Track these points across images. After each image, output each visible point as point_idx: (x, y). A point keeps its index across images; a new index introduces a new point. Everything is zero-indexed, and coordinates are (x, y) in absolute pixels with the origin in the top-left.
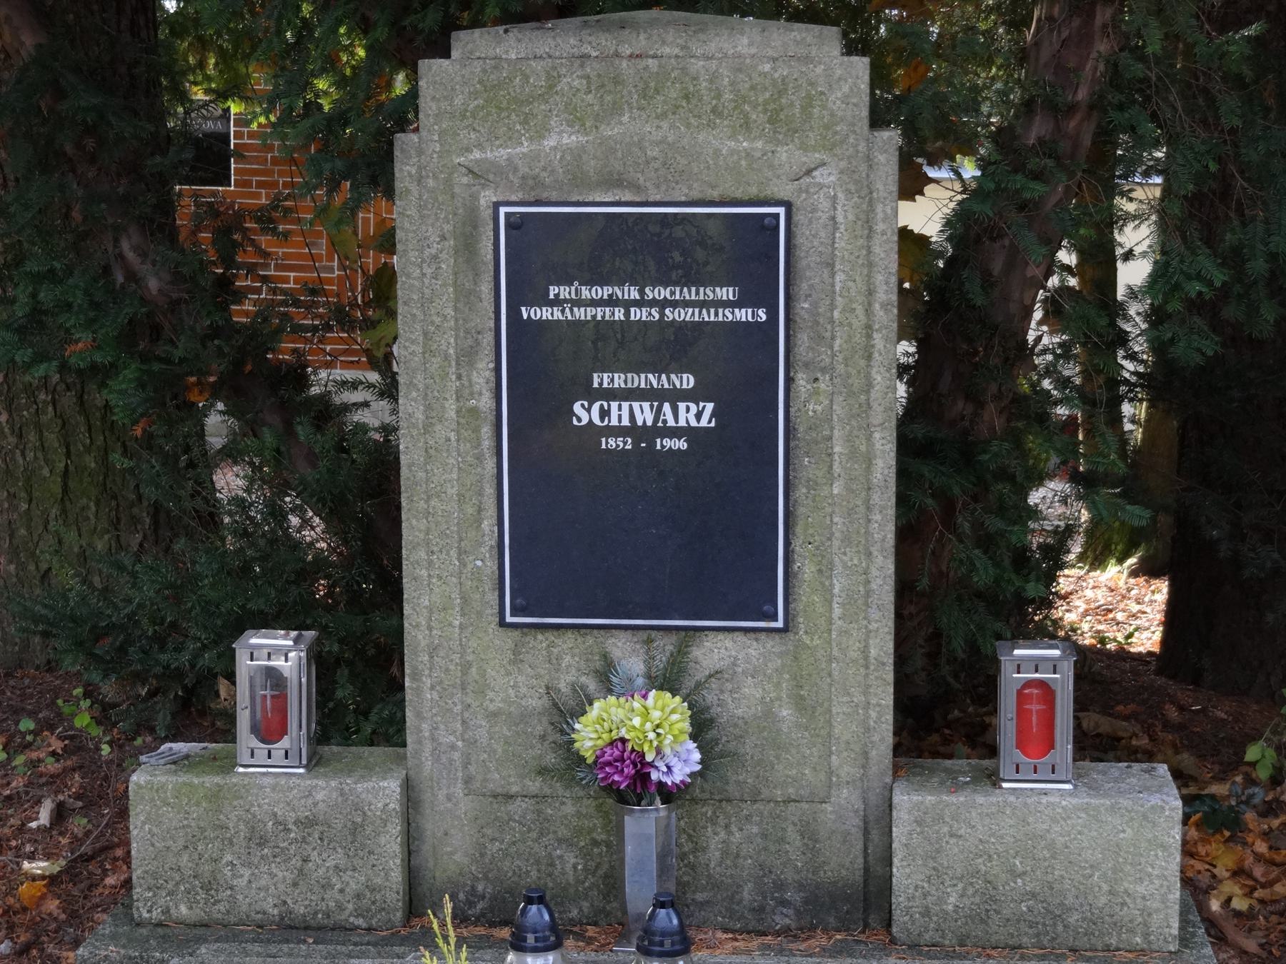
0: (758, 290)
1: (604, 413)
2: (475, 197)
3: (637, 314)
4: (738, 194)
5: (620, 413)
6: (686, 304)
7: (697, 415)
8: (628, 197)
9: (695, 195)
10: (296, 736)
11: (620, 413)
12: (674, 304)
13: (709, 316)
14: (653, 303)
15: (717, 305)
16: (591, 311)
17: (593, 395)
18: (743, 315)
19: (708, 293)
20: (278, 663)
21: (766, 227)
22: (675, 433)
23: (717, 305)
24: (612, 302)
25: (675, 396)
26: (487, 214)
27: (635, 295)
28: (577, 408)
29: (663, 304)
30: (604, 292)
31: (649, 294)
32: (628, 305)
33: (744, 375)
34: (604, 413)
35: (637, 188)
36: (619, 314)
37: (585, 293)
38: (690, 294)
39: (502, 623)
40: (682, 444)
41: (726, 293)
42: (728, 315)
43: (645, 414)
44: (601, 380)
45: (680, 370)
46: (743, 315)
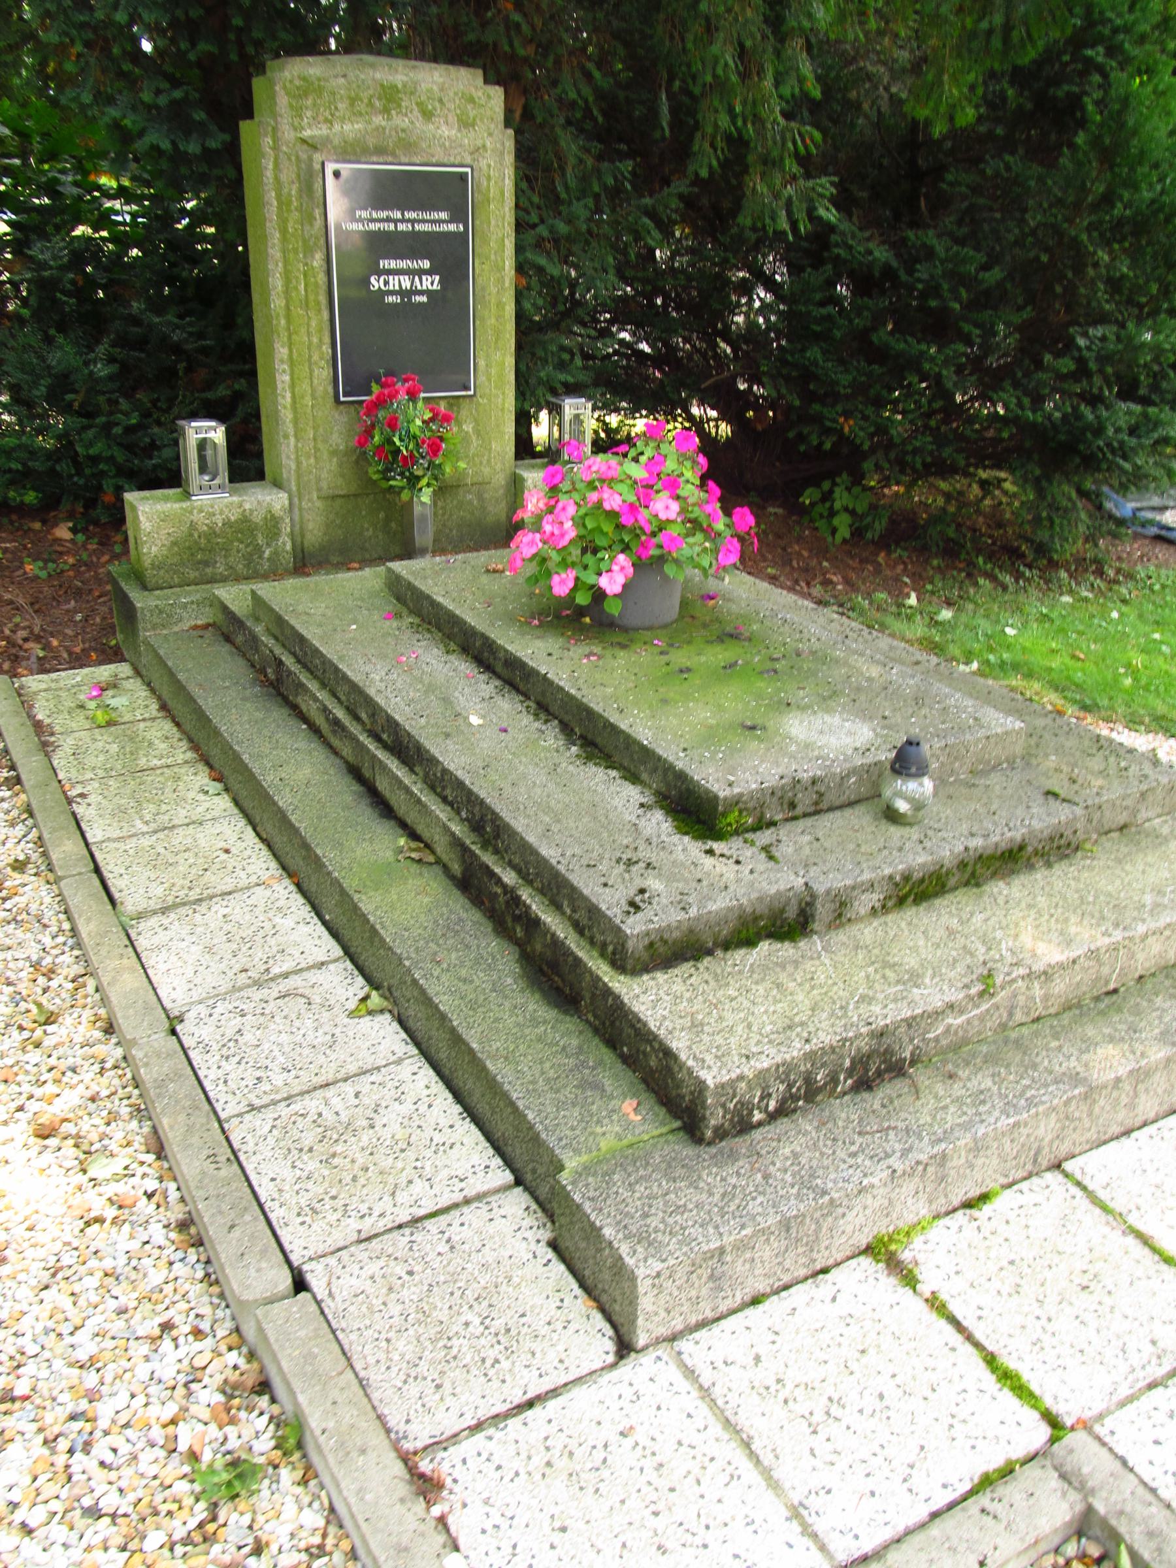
0: (459, 214)
1: (386, 283)
2: (311, 159)
3: (402, 227)
4: (445, 161)
5: (394, 283)
6: (424, 221)
7: (431, 283)
8: (390, 159)
9: (425, 160)
10: (223, 476)
11: (394, 283)
12: (419, 221)
13: (436, 228)
14: (409, 221)
15: (436, 222)
16: (378, 225)
17: (380, 273)
18: (452, 227)
19: (435, 215)
20: (211, 435)
21: (463, 177)
22: (421, 293)
23: (436, 222)
24: (388, 220)
25: (421, 272)
26: (318, 167)
27: (399, 216)
28: (373, 280)
29: (413, 222)
30: (383, 214)
31: (407, 215)
32: (396, 221)
33: (450, 258)
34: (386, 283)
35: (393, 154)
36: (392, 227)
37: (374, 215)
38: (427, 216)
39: (337, 401)
40: (424, 299)
41: (443, 215)
42: (445, 228)
43: (406, 283)
44: (385, 264)
45: (422, 258)
46: (452, 227)
